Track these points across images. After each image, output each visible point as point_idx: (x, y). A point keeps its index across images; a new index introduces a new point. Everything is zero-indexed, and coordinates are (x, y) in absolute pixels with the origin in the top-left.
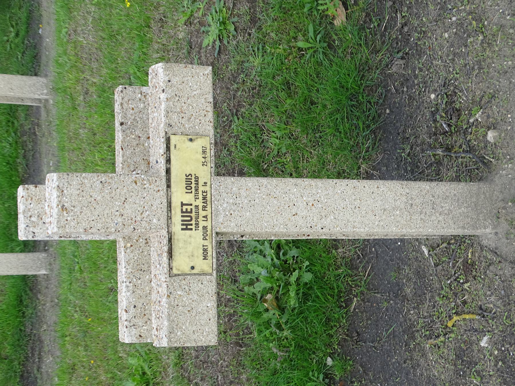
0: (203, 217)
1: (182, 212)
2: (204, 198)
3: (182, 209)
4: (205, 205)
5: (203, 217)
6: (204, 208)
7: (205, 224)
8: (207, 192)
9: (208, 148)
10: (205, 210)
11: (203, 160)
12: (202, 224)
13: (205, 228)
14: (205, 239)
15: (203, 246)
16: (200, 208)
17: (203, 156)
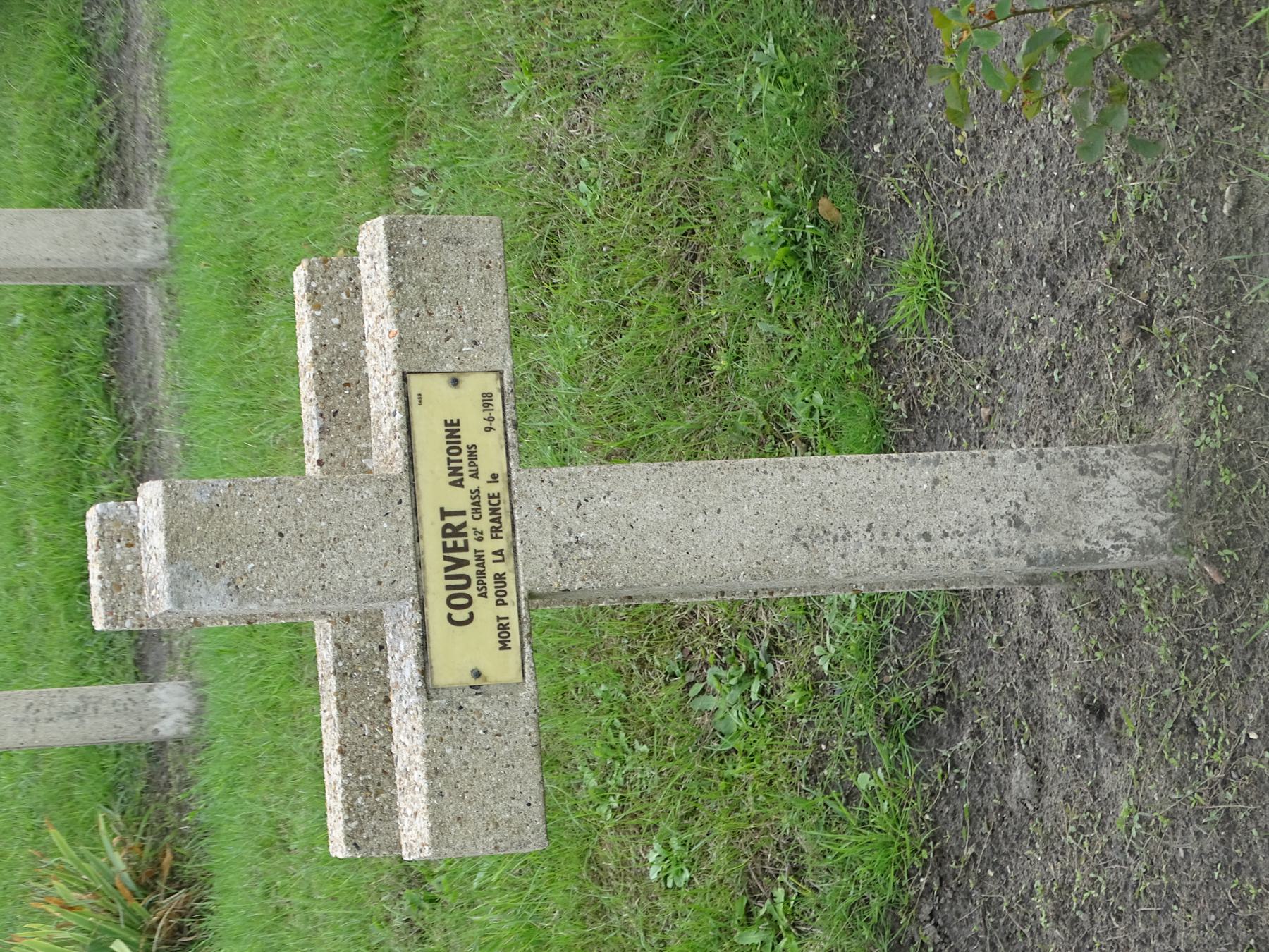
0: (495, 553)
1: (445, 549)
2: (494, 510)
3: (444, 543)
4: (497, 525)
5: (495, 553)
6: (496, 532)
7: (500, 568)
8: (498, 497)
9: (497, 401)
10: (497, 537)
11: (487, 424)
12: (492, 569)
13: (499, 578)
14: (501, 602)
15: (499, 618)
16: (487, 535)
17: (486, 415)
